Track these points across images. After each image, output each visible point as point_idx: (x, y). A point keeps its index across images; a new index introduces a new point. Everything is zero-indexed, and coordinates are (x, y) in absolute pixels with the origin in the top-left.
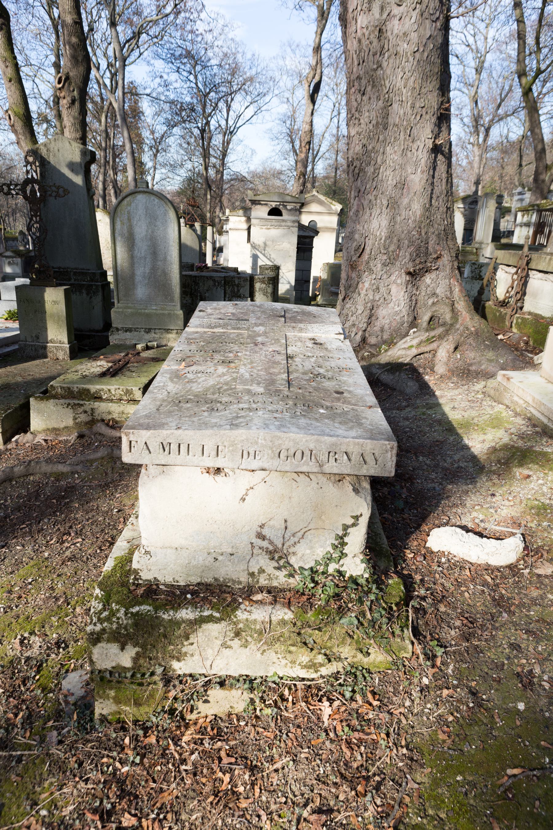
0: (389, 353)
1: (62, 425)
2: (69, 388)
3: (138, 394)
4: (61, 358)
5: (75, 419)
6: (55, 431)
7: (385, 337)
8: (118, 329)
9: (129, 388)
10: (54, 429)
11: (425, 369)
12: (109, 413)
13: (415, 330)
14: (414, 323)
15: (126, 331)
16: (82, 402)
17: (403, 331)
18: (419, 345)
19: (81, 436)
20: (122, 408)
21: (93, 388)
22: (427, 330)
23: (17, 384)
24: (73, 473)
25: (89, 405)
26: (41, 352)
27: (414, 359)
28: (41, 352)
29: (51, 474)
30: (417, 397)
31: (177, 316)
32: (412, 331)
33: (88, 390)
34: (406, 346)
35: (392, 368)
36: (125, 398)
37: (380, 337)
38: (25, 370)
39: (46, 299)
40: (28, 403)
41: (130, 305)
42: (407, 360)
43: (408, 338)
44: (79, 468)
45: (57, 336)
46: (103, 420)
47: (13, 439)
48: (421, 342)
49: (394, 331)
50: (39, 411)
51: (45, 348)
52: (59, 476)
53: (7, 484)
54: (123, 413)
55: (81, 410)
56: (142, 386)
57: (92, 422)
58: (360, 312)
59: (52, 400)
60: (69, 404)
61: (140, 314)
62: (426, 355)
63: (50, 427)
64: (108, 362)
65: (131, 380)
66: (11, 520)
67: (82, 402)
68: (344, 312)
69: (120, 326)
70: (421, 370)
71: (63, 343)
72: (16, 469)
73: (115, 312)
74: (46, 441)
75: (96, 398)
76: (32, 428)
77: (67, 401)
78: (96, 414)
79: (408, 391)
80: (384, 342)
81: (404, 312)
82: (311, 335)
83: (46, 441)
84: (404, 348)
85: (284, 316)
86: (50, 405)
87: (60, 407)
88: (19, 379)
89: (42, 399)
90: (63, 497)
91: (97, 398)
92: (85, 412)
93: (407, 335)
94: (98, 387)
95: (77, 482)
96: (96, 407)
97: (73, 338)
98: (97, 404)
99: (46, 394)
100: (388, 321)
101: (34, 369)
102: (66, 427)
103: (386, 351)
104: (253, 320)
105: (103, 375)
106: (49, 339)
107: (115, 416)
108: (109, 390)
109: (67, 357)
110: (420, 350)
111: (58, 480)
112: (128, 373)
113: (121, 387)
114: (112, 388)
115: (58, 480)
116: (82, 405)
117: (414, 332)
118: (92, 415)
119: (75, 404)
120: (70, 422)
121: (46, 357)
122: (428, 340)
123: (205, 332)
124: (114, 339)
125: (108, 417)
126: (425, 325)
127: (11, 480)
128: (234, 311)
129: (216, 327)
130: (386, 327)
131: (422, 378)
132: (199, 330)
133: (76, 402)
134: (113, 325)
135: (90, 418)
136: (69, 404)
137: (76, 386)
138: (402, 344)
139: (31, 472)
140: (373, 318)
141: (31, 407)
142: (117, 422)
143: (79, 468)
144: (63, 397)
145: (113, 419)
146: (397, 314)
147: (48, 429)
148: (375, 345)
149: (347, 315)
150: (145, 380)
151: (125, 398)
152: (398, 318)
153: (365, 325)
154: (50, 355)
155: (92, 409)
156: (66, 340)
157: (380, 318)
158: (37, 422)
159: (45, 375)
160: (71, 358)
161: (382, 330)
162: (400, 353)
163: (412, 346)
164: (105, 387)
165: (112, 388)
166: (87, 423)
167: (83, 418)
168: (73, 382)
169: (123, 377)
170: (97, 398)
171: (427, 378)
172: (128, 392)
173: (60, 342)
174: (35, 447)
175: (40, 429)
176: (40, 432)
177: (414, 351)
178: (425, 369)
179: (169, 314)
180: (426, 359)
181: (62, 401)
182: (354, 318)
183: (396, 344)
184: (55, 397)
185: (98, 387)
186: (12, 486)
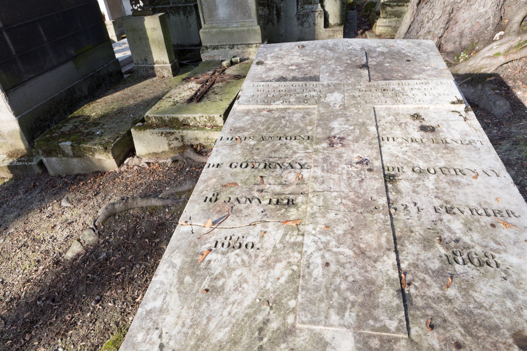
0: (471, 63)
1: (160, 150)
2: (161, 118)
3: (219, 121)
4: (166, 76)
5: (169, 145)
6: (155, 154)
7: (464, 43)
8: (207, 48)
9: (211, 116)
10: (155, 154)
11: (515, 81)
12: (197, 139)
13: (502, 33)
14: (499, 26)
15: (214, 49)
16: (172, 131)
17: (487, 37)
18: (507, 52)
19: (175, 161)
20: (206, 135)
21: (181, 117)
22: (519, 34)
23: (129, 108)
24: (164, 207)
25: (179, 133)
26: (150, 72)
27: (500, 69)
28: (150, 72)
29: (147, 208)
30: (509, 120)
31: (255, 31)
32: (497, 35)
33: (177, 119)
34: (491, 54)
35: (472, 80)
36: (209, 124)
37: (457, 44)
38: (137, 91)
39: (146, 27)
40: (129, 133)
41: (214, 25)
42: (491, 70)
43: (494, 44)
44: (169, 202)
45: (161, 57)
46: (192, 146)
47: (125, 162)
48: (510, 49)
49: (476, 35)
50: (140, 139)
51: (153, 68)
52: (154, 210)
53: (111, 219)
54: (208, 139)
55: (172, 137)
56: (222, 112)
57: (183, 147)
58: (437, 17)
59: (148, 130)
60: (162, 133)
61: (224, 32)
62: (515, 63)
63: (151, 152)
64: (197, 83)
65: (214, 105)
66: (111, 263)
67: (172, 131)
68: (418, 18)
69: (208, 45)
70: (510, 83)
71: (166, 63)
72: (117, 206)
73: (205, 33)
74: (148, 164)
75: (184, 125)
76: (138, 152)
77: (161, 131)
78: (186, 140)
79: (497, 111)
80: (463, 49)
81: (490, 14)
82: (411, 108)
83: (148, 164)
84: (489, 57)
85: (366, 66)
86: (148, 134)
87: (155, 136)
88: (131, 102)
89: (140, 130)
90: (155, 237)
91: (185, 125)
92: (177, 139)
93: (491, 40)
94: (185, 116)
95: (168, 217)
96: (184, 134)
97: (174, 57)
98: (185, 132)
99: (144, 124)
100: (469, 25)
101: (143, 89)
102: (163, 152)
103: (466, 60)
104: (325, 79)
105: (191, 100)
106: (155, 60)
107: (202, 141)
108: (195, 118)
109: (171, 75)
110: (508, 59)
111: (151, 214)
112: (212, 96)
113: (204, 115)
114: (197, 116)
115: (151, 214)
116: (173, 133)
117: (501, 37)
118: (182, 141)
119: (167, 133)
120: (166, 148)
121: (155, 76)
122: (520, 45)
123: (260, 111)
124: (205, 56)
125: (195, 143)
126: (515, 26)
127: (114, 215)
128: (300, 61)
129: (274, 99)
130: (467, 31)
131: (514, 94)
132: (251, 107)
133: (168, 131)
134: (203, 44)
135: (181, 144)
136: (162, 133)
137: (166, 115)
138: (486, 52)
139: (130, 207)
140: (452, 22)
141: (134, 137)
142: (204, 147)
143: (169, 202)
144: (158, 126)
145: (201, 145)
146: (481, 16)
147: (150, 154)
148: (452, 52)
149: (422, 21)
150: (226, 105)
151: (209, 124)
152: (481, 21)
153: (442, 30)
154: (158, 74)
155: (182, 137)
156: (167, 61)
157: (460, 22)
158: (140, 148)
159: (152, 95)
160: (174, 75)
161: (461, 35)
162: (484, 62)
163: (498, 54)
164: (191, 116)
165: (197, 116)
166: (179, 148)
167: (176, 144)
168: (164, 112)
169: (208, 102)
170: (185, 125)
171: (519, 94)
172: (211, 119)
173: (164, 63)
174: (140, 170)
175: (143, 154)
176: (144, 156)
177: (502, 59)
178: (515, 81)
179: (248, 30)
180: (515, 68)
181: (156, 130)
182: (430, 24)
183: (478, 51)
184: (151, 127)
185: (185, 116)
186: (116, 221)
